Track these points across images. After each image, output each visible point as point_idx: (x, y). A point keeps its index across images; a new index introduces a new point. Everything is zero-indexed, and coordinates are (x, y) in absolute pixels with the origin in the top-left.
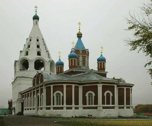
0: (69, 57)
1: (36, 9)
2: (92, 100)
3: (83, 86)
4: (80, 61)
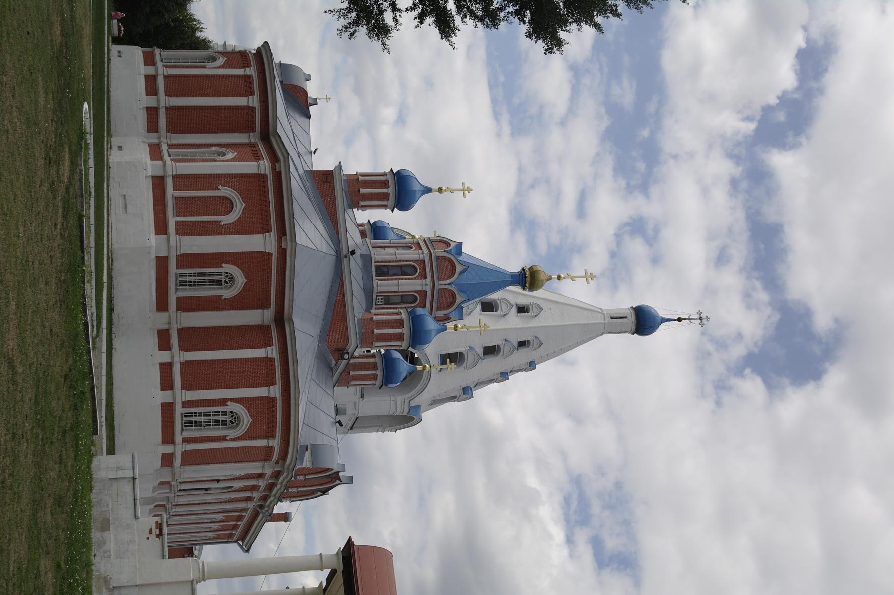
0: (398, 172)
1: (689, 319)
4: (392, 257)
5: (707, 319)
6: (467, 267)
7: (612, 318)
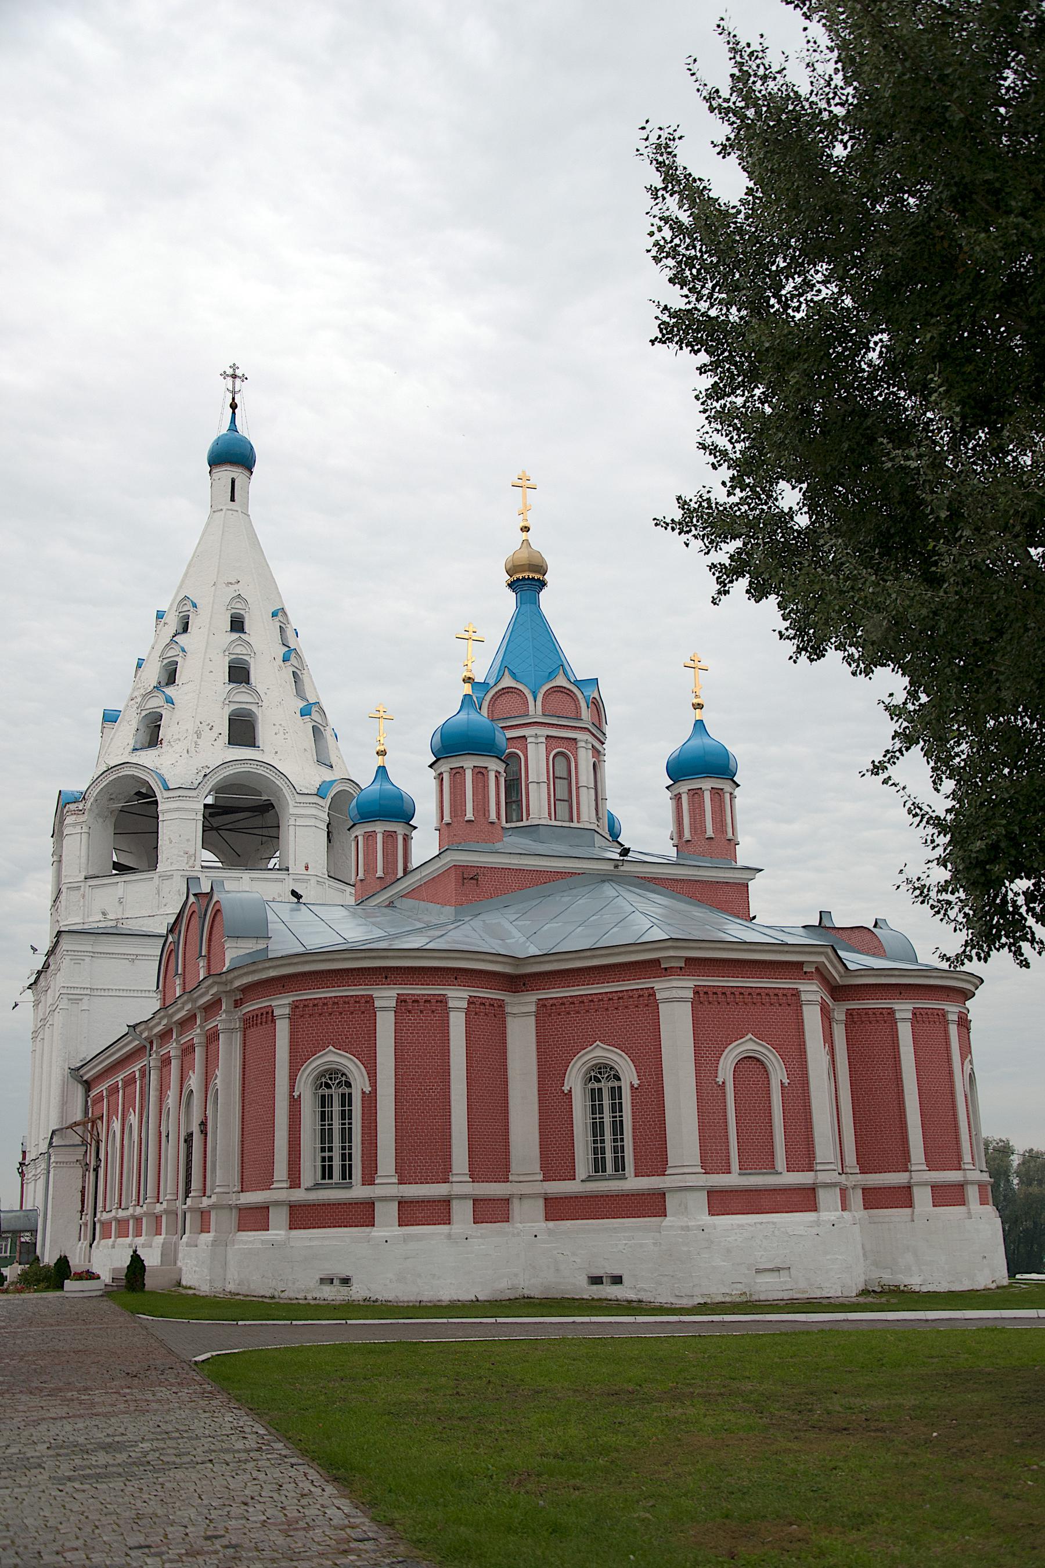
1: (234, 393)
2: (618, 1127)
3: (541, 1004)
5: (234, 367)
6: (505, 668)
7: (233, 499)
